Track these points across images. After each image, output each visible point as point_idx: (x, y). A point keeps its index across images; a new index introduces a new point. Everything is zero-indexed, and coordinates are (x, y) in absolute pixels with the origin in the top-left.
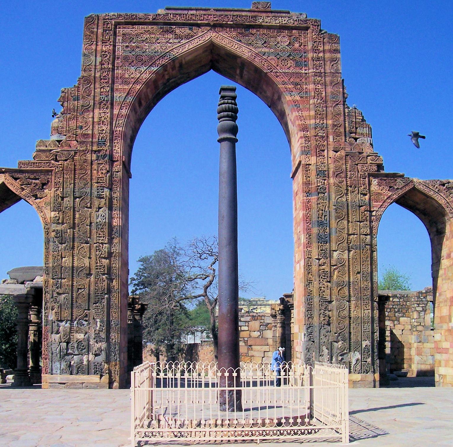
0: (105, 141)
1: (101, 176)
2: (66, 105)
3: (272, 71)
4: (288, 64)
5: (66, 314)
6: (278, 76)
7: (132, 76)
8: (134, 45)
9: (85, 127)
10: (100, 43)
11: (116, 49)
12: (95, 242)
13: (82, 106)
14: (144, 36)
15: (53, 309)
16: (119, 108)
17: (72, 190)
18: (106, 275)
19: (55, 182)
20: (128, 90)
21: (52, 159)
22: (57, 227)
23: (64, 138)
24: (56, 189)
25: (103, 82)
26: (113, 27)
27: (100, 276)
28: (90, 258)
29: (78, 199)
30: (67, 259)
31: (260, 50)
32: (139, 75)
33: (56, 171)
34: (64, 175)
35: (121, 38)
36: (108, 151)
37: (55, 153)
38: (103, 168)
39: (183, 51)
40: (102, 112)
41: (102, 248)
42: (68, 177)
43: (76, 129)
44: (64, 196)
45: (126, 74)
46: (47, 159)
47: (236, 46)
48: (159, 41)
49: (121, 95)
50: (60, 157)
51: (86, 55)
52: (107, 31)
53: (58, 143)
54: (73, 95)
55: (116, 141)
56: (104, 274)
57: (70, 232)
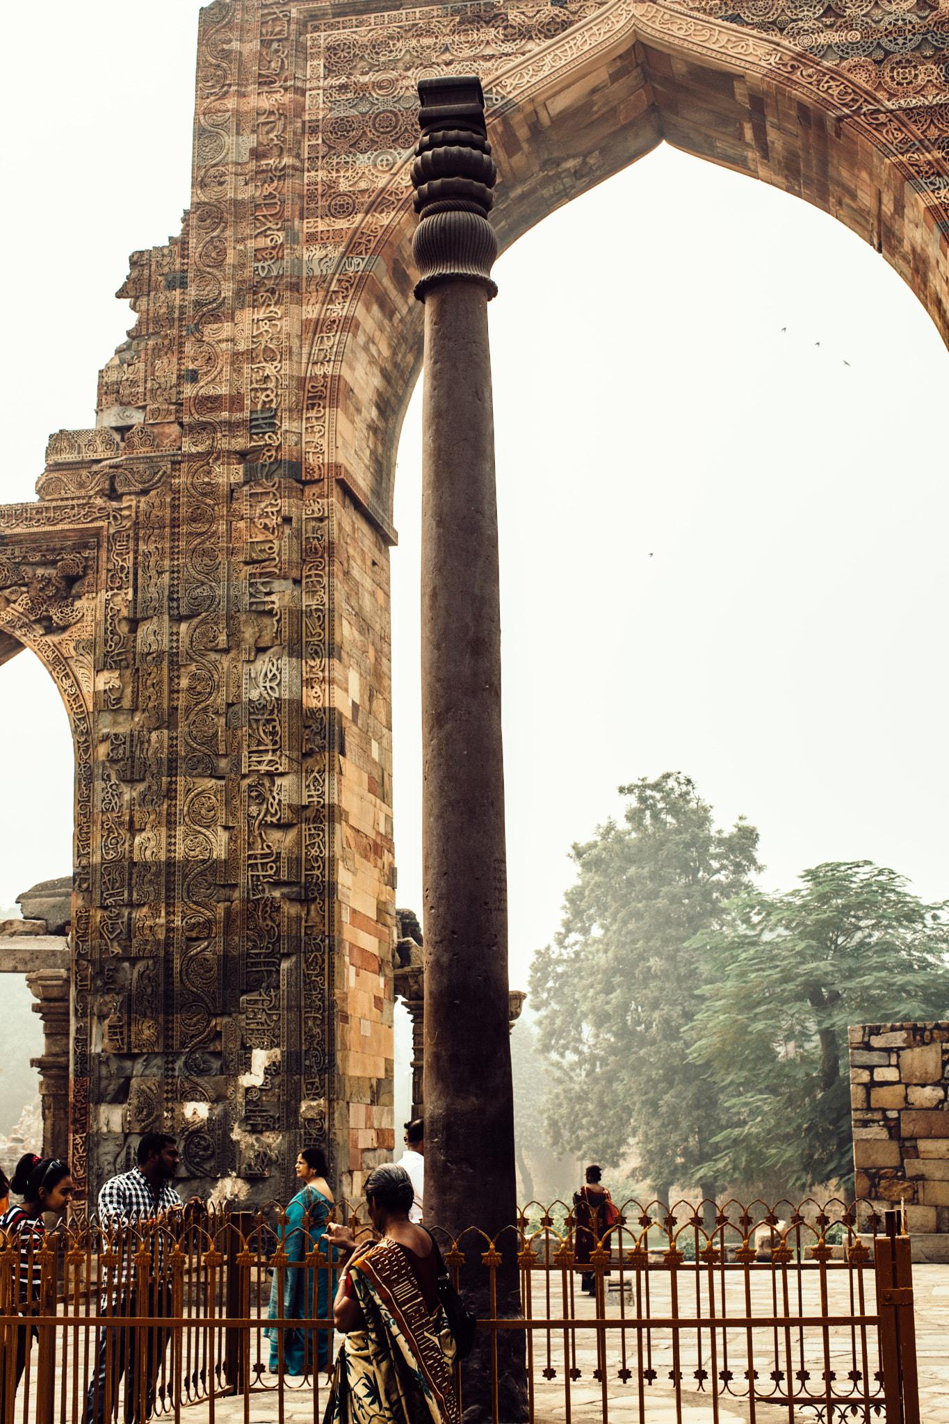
0: (271, 417)
1: (260, 538)
2: (143, 308)
3: (860, 108)
4: (916, 75)
5: (147, 1031)
6: (884, 124)
7: (363, 185)
8: (365, 79)
9: (206, 374)
10: (250, 88)
11: (308, 102)
12: (244, 771)
13: (198, 304)
14: (399, 45)
15: (102, 1017)
16: (321, 298)
17: (166, 593)
18: (285, 890)
19: (109, 571)
20: (350, 232)
21: (97, 493)
22: (115, 723)
23: (137, 418)
24: (110, 593)
25: (264, 216)
26: (293, 27)
27: (263, 891)
28: (226, 828)
29: (184, 627)
30: (150, 835)
31: (807, 41)
32: (388, 176)
33: (112, 531)
34: (137, 545)
35: (322, 62)
36: (285, 447)
37: (107, 470)
38: (269, 509)
39: (533, 81)
40: (261, 316)
41: (271, 791)
42: (152, 547)
43: (178, 385)
44: (139, 616)
45: (342, 180)
46: (83, 493)
47: (724, 38)
48: (447, 57)
49: (324, 253)
50: (127, 482)
51: (204, 130)
52: (275, 45)
53: (117, 437)
54: (166, 270)
55: (312, 414)
56: (277, 884)
57: (160, 741)
